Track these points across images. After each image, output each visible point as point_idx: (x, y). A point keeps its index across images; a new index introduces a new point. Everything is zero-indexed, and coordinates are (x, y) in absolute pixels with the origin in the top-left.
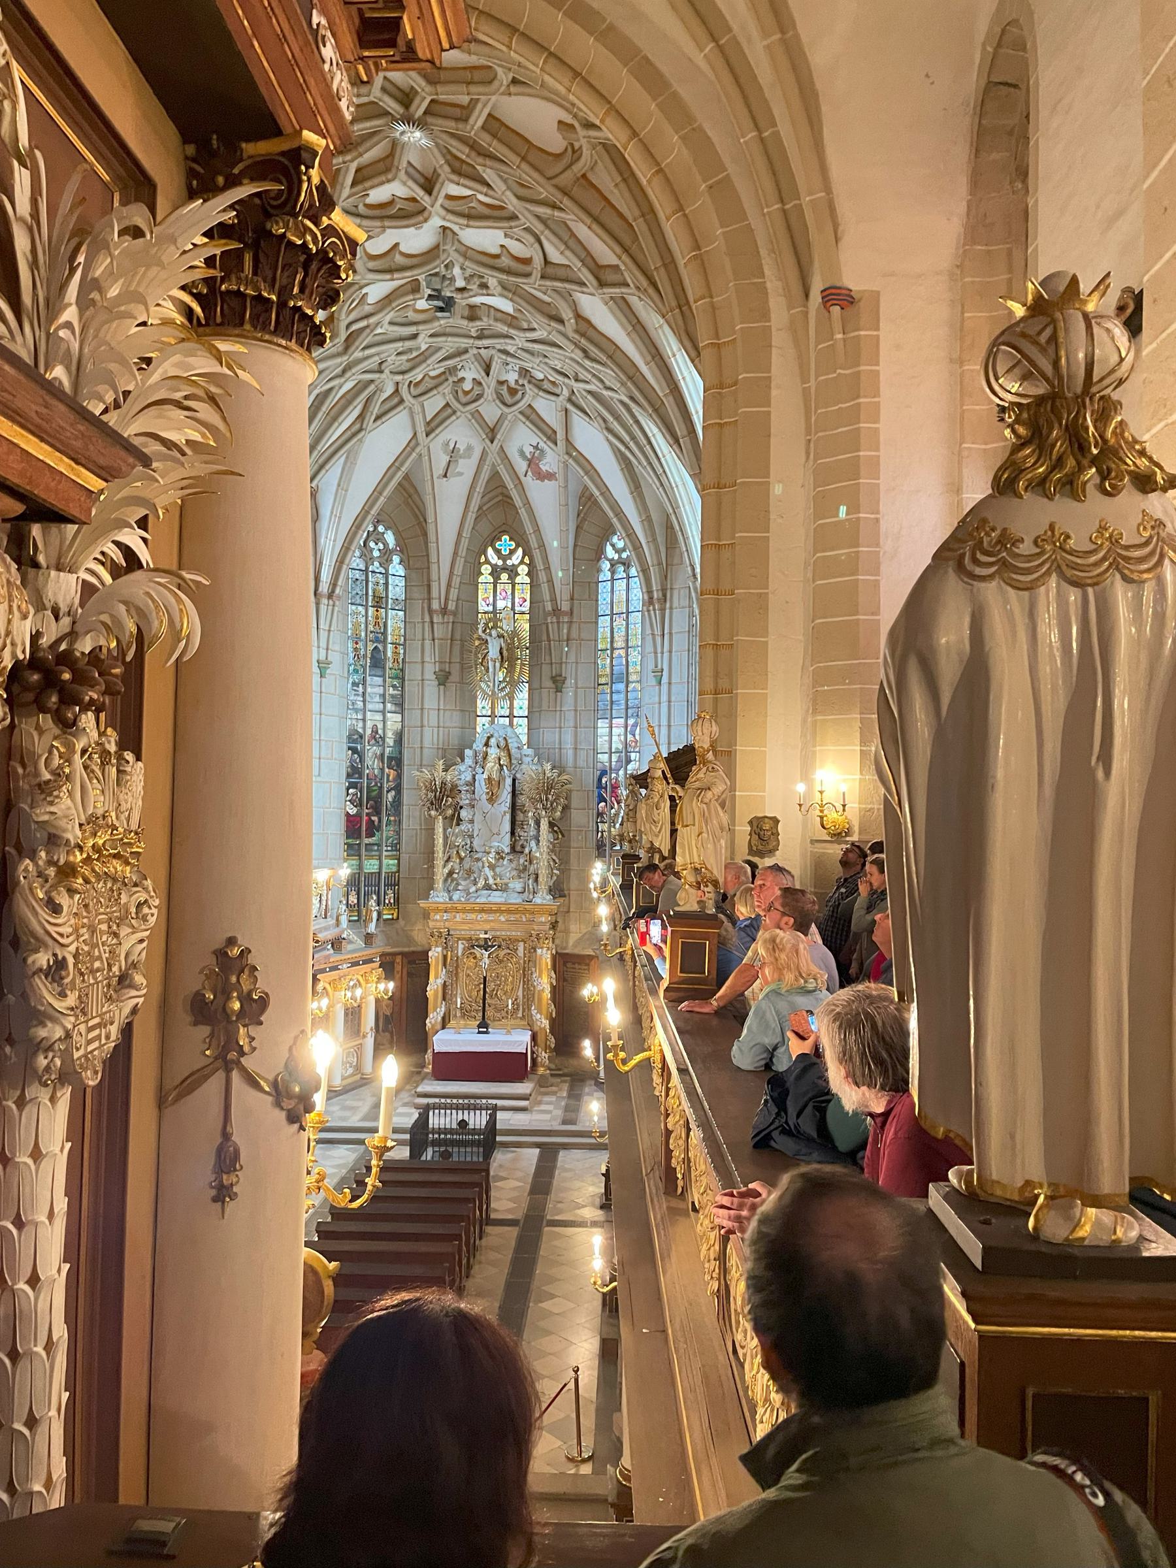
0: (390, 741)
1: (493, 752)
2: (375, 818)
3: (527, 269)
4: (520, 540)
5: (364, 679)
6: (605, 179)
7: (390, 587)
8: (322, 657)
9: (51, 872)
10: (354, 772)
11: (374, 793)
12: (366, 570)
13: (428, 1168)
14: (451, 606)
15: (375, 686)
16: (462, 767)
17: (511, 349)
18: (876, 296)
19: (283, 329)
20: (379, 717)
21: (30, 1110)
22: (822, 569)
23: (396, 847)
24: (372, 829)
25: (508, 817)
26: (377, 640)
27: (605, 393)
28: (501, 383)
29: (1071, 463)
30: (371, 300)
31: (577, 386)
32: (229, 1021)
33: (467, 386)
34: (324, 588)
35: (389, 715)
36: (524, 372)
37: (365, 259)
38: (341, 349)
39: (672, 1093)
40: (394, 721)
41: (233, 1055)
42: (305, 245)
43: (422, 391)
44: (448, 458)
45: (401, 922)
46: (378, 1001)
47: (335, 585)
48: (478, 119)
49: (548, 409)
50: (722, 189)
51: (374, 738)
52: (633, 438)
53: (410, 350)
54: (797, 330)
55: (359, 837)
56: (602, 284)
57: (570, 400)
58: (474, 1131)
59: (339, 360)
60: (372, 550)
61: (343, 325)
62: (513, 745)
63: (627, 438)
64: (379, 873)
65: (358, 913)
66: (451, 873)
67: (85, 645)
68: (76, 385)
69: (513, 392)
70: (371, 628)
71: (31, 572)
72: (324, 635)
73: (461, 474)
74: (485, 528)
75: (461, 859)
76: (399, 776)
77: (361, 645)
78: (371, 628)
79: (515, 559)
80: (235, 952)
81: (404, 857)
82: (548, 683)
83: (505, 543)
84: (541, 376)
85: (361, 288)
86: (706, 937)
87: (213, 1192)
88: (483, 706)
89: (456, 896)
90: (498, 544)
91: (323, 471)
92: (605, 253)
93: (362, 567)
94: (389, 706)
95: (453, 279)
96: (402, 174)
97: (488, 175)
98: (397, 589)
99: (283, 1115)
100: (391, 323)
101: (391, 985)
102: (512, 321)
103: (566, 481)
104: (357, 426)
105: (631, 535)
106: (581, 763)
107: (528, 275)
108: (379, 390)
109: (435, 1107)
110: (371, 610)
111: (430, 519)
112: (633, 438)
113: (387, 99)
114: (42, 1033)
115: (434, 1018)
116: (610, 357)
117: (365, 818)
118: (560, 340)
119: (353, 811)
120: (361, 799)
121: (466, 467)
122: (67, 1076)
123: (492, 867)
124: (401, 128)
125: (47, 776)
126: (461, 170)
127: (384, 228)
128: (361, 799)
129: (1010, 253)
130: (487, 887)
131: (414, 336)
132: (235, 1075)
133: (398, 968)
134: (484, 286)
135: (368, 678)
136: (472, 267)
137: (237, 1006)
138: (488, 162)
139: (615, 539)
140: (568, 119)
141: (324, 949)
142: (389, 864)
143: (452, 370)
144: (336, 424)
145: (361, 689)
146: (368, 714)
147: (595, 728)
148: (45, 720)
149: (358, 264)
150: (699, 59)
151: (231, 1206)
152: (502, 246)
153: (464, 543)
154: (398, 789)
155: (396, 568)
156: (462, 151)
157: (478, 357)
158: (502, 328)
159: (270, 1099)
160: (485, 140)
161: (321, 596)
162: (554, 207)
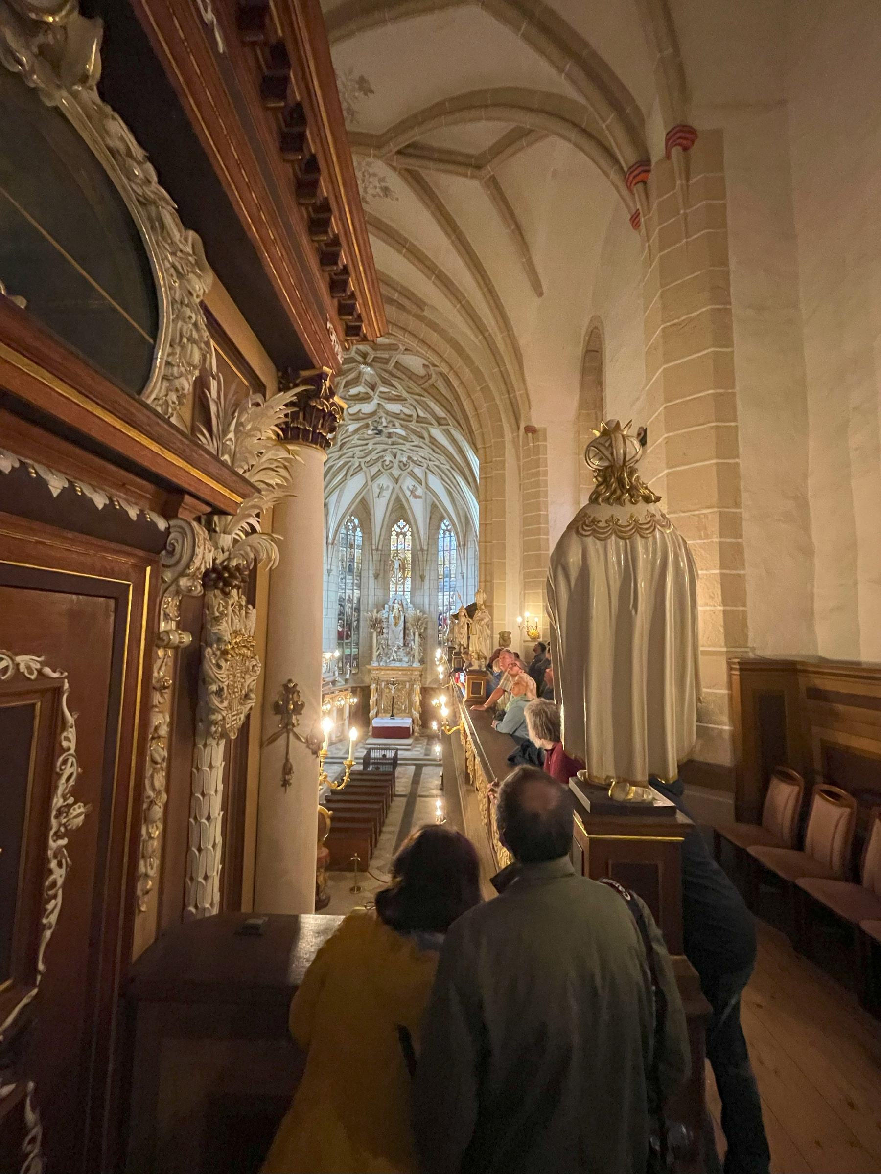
0: (355, 601)
1: (396, 606)
2: (349, 632)
3: (410, 419)
4: (408, 522)
5: (345, 578)
6: (441, 385)
8: (329, 568)
9: (218, 653)
10: (341, 613)
13: (370, 774)
14: (380, 548)
16: (384, 612)
17: (405, 449)
18: (545, 430)
19: (314, 441)
20: (351, 592)
21: (208, 749)
22: (525, 533)
23: (357, 644)
24: (348, 637)
25: (402, 632)
26: (351, 561)
27: (441, 466)
28: (400, 462)
29: (619, 492)
31: (428, 462)
32: (289, 713)
33: (387, 463)
34: (330, 541)
36: (409, 458)
38: (338, 449)
39: (468, 743)
41: (290, 727)
42: (323, 410)
43: (370, 465)
44: (378, 491)
45: (360, 675)
46: (350, 706)
48: (392, 363)
49: (418, 471)
50: (485, 390)
52: (452, 482)
53: (365, 450)
54: (515, 442)
55: (343, 640)
56: (440, 424)
57: (427, 468)
58: (389, 759)
59: (337, 453)
61: (339, 440)
62: (404, 603)
63: (449, 482)
65: (342, 672)
66: (379, 655)
67: (234, 563)
68: (233, 462)
69: (405, 465)
70: (348, 556)
71: (214, 534)
72: (330, 559)
73: (384, 496)
74: (394, 516)
75: (383, 649)
76: (359, 616)
77: (344, 563)
79: (405, 530)
80: (292, 685)
82: (418, 578)
83: (402, 523)
84: (415, 459)
86: (482, 680)
87: (282, 783)
88: (392, 587)
89: (381, 664)
90: (399, 524)
92: (440, 412)
93: (345, 532)
94: (355, 587)
95: (382, 423)
96: (363, 384)
97: (395, 383)
99: (310, 752)
100: (358, 439)
102: (405, 439)
103: (426, 499)
105: (451, 519)
106: (432, 609)
107: (411, 421)
108: (353, 464)
109: (373, 749)
111: (372, 514)
112: (452, 482)
113: (357, 355)
114: (213, 717)
115: (373, 713)
116: (443, 452)
118: (424, 446)
119: (340, 629)
121: (386, 494)
122: (224, 735)
123: (396, 652)
124: (362, 366)
125: (217, 614)
126: (386, 382)
127: (355, 404)
129: (596, 414)
130: (394, 660)
131: (367, 444)
132: (291, 735)
133: (358, 692)
134: (394, 425)
136: (389, 418)
137: (292, 707)
138: (396, 379)
139: (445, 521)
140: (427, 363)
142: (355, 651)
143: (382, 457)
146: (347, 591)
147: (437, 595)
148: (217, 592)
149: (346, 418)
150: (476, 341)
151: (288, 788)
152: (401, 411)
153: (385, 523)
154: (358, 620)
155: (359, 533)
156: (386, 375)
157: (391, 452)
158: (401, 441)
159: (305, 745)
160: (395, 371)
162: (421, 395)
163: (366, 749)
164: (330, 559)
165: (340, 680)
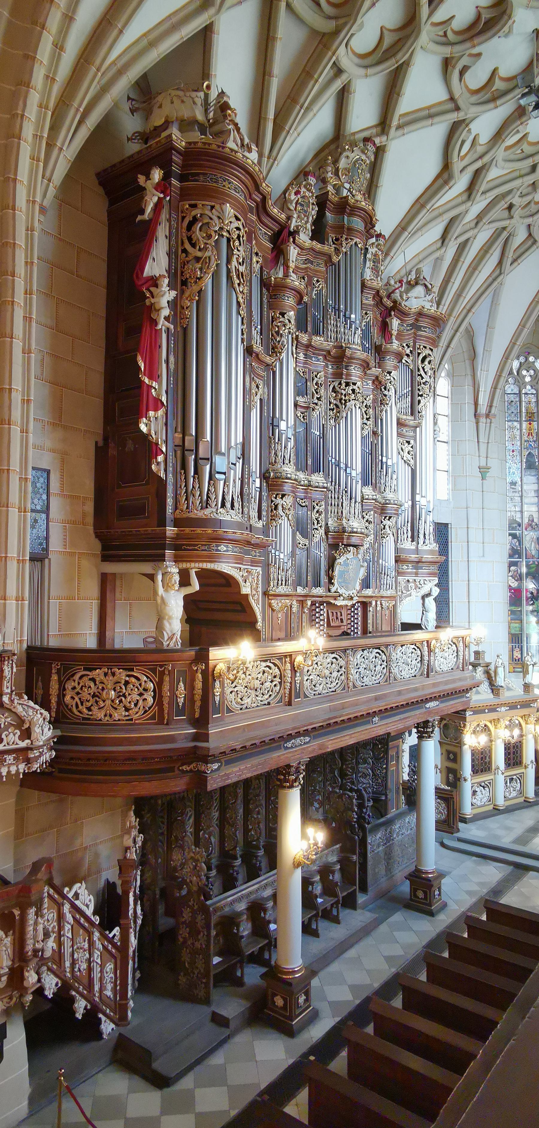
8: (483, 464)
10: (515, 552)
30: (484, 139)
34: (483, 409)
37: (468, 95)
47: (491, 406)
51: (531, 525)
55: (520, 605)
70: (525, 438)
72: (483, 447)
85: (467, 125)
91: (470, 314)
104: (497, 272)
119: (515, 584)
141: (463, 697)
144: (477, 272)
146: (525, 508)
149: (461, 103)
161: (479, 416)
164: (483, 447)
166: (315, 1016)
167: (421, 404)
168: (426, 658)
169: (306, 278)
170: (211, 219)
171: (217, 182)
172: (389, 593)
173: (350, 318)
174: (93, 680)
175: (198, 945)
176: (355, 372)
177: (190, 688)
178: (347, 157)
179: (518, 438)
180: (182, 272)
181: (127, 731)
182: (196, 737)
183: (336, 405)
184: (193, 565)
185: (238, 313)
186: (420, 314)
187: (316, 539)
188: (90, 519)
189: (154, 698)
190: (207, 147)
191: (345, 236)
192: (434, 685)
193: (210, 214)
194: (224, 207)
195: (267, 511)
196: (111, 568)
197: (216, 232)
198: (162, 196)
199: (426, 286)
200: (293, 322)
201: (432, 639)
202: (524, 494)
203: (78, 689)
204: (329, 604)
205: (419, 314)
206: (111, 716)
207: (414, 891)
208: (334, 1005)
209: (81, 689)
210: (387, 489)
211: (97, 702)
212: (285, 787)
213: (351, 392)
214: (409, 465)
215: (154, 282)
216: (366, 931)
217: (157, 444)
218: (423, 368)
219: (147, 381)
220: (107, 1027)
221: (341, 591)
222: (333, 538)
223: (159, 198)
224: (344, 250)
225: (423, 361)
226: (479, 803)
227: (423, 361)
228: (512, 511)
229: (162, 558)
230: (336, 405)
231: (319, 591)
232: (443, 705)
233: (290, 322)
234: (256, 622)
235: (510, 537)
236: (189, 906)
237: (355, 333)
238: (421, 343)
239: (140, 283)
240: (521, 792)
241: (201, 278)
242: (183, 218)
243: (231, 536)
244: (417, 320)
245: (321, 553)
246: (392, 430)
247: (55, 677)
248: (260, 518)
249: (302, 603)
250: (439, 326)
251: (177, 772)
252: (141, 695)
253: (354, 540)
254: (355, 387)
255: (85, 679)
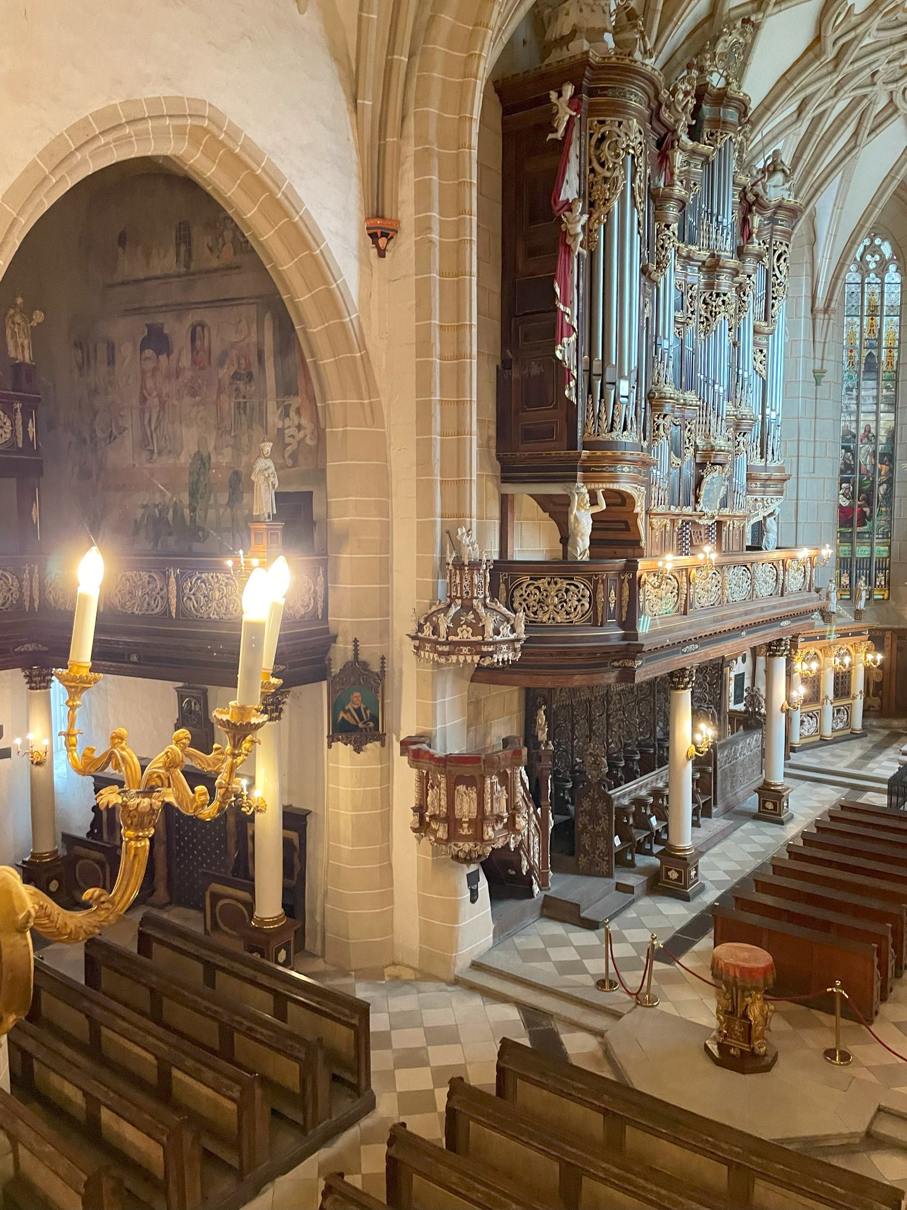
0: (883, 439)
2: (867, 510)
5: (858, 384)
7: (886, 295)
10: (848, 468)
11: (867, 487)
12: (862, 283)
15: (868, 389)
20: (872, 417)
23: (887, 535)
26: (871, 347)
34: (820, 303)
35: (882, 415)
40: (887, 420)
46: (867, 669)
55: (851, 526)
60: (868, 263)
64: (871, 558)
65: (850, 594)
72: (819, 347)
76: (892, 471)
78: (866, 336)
81: (895, 544)
91: (819, 194)
94: (882, 406)
98: (893, 296)
101: (880, 657)
104: (852, 144)
110: (866, 320)
117: (857, 509)
119: (845, 503)
120: (853, 493)
128: (853, 493)
133: (888, 642)
135: (862, 383)
141: (809, 618)
142: (881, 550)
144: (831, 146)
145: (855, 393)
146: (862, 416)
154: (890, 482)
155: (893, 276)
161: (818, 311)
163: (900, 762)
164: (819, 347)
165: (843, 611)
166: (702, 889)
167: (775, 308)
168: (781, 577)
169: (684, 182)
170: (619, 136)
171: (625, 96)
172: (740, 513)
173: (722, 222)
174: (538, 588)
175: (599, 829)
176: (724, 282)
177: (620, 595)
178: (726, 41)
179: (858, 335)
180: (590, 194)
181: (571, 632)
182: (624, 637)
183: (706, 318)
184: (601, 485)
185: (639, 233)
186: (779, 206)
187: (687, 459)
188: (493, 443)
189: (590, 603)
190: (620, 61)
191: (720, 131)
192: (789, 604)
193: (617, 130)
194: (630, 122)
195: (650, 432)
196: (509, 489)
197: (623, 149)
198: (574, 114)
199: (783, 171)
200: (676, 233)
201: (788, 558)
202: (862, 401)
203: (525, 596)
204: (694, 523)
205: (779, 206)
206: (554, 619)
207: (762, 804)
208: (717, 884)
209: (528, 595)
210: (743, 403)
211: (541, 607)
212: (678, 689)
213: (721, 303)
214: (761, 376)
215: (569, 206)
216: (724, 835)
217: (569, 370)
218: (778, 267)
219: (562, 307)
220: (536, 889)
221: (705, 510)
222: (702, 457)
223: (571, 116)
224: (719, 146)
225: (778, 259)
226: (806, 734)
227: (778, 259)
228: (847, 422)
229: (574, 480)
230: (706, 318)
231: (688, 510)
232: (793, 625)
233: (674, 234)
234: (640, 540)
235: (843, 451)
236: (589, 797)
237: (727, 239)
238: (778, 238)
239: (557, 208)
240: (848, 724)
241: (609, 199)
242: (591, 135)
243: (629, 458)
244: (775, 213)
245: (689, 471)
246: (748, 337)
247: (502, 586)
248: (645, 439)
249: (673, 521)
250: (796, 217)
251: (609, 667)
252: (579, 601)
253: (719, 459)
254: (725, 298)
255: (532, 587)
